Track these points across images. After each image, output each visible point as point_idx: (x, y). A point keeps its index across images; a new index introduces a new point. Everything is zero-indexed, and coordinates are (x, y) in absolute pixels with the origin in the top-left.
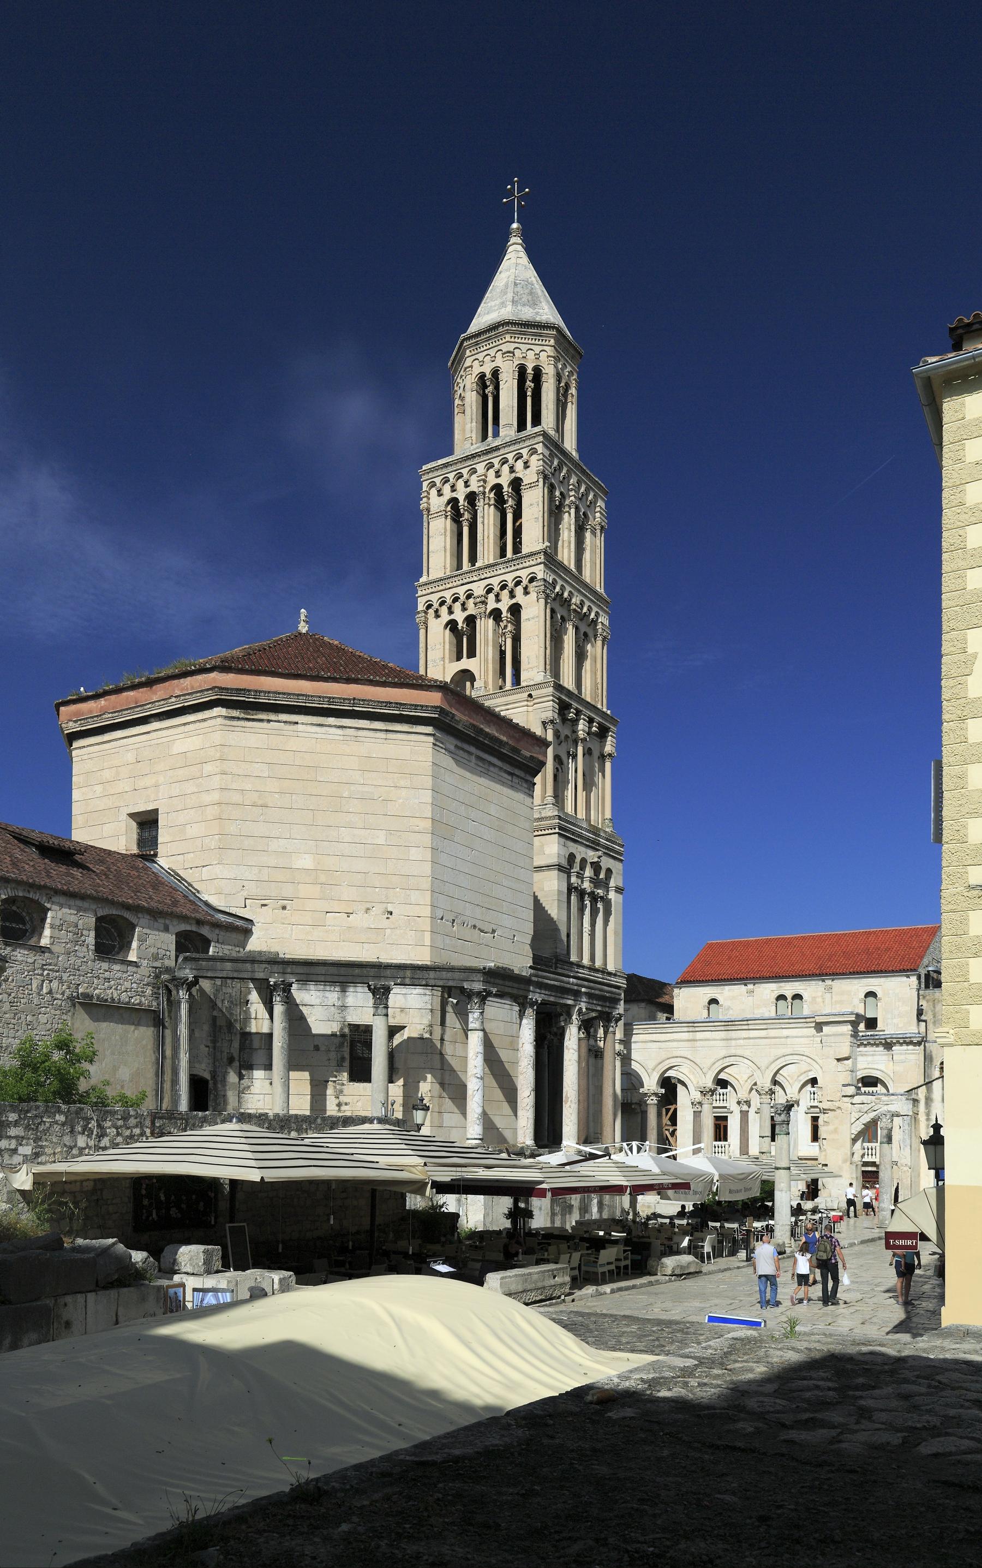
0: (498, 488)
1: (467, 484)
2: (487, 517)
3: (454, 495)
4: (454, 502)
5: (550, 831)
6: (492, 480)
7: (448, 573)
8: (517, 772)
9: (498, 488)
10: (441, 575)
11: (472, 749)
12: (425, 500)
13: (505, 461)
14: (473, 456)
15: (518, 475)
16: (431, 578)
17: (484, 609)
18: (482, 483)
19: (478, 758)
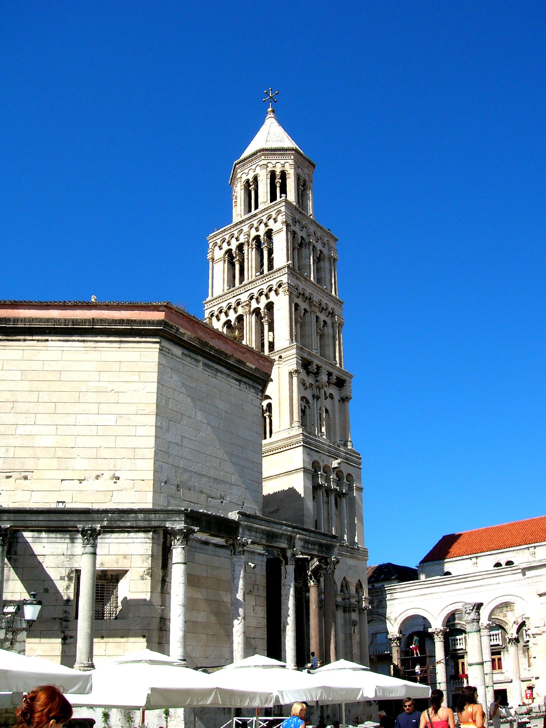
0: (257, 238)
1: (237, 239)
2: (251, 255)
3: (229, 247)
4: (229, 252)
5: (297, 445)
6: (253, 233)
7: (226, 291)
8: (244, 379)
9: (257, 238)
10: (221, 293)
11: (200, 358)
12: (210, 253)
13: (261, 222)
14: (241, 222)
15: (269, 228)
16: (215, 296)
17: (248, 309)
18: (246, 236)
19: (205, 365)
